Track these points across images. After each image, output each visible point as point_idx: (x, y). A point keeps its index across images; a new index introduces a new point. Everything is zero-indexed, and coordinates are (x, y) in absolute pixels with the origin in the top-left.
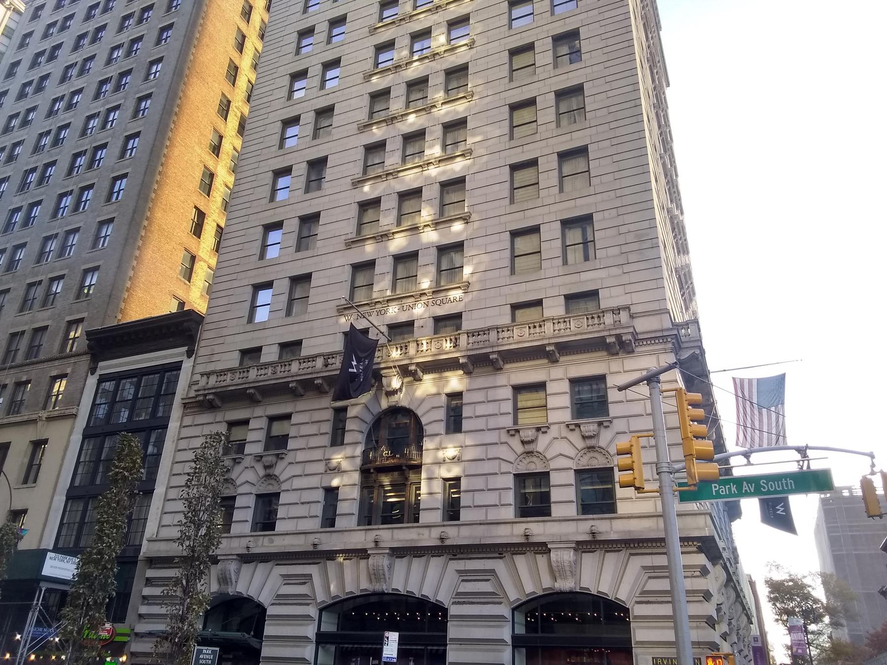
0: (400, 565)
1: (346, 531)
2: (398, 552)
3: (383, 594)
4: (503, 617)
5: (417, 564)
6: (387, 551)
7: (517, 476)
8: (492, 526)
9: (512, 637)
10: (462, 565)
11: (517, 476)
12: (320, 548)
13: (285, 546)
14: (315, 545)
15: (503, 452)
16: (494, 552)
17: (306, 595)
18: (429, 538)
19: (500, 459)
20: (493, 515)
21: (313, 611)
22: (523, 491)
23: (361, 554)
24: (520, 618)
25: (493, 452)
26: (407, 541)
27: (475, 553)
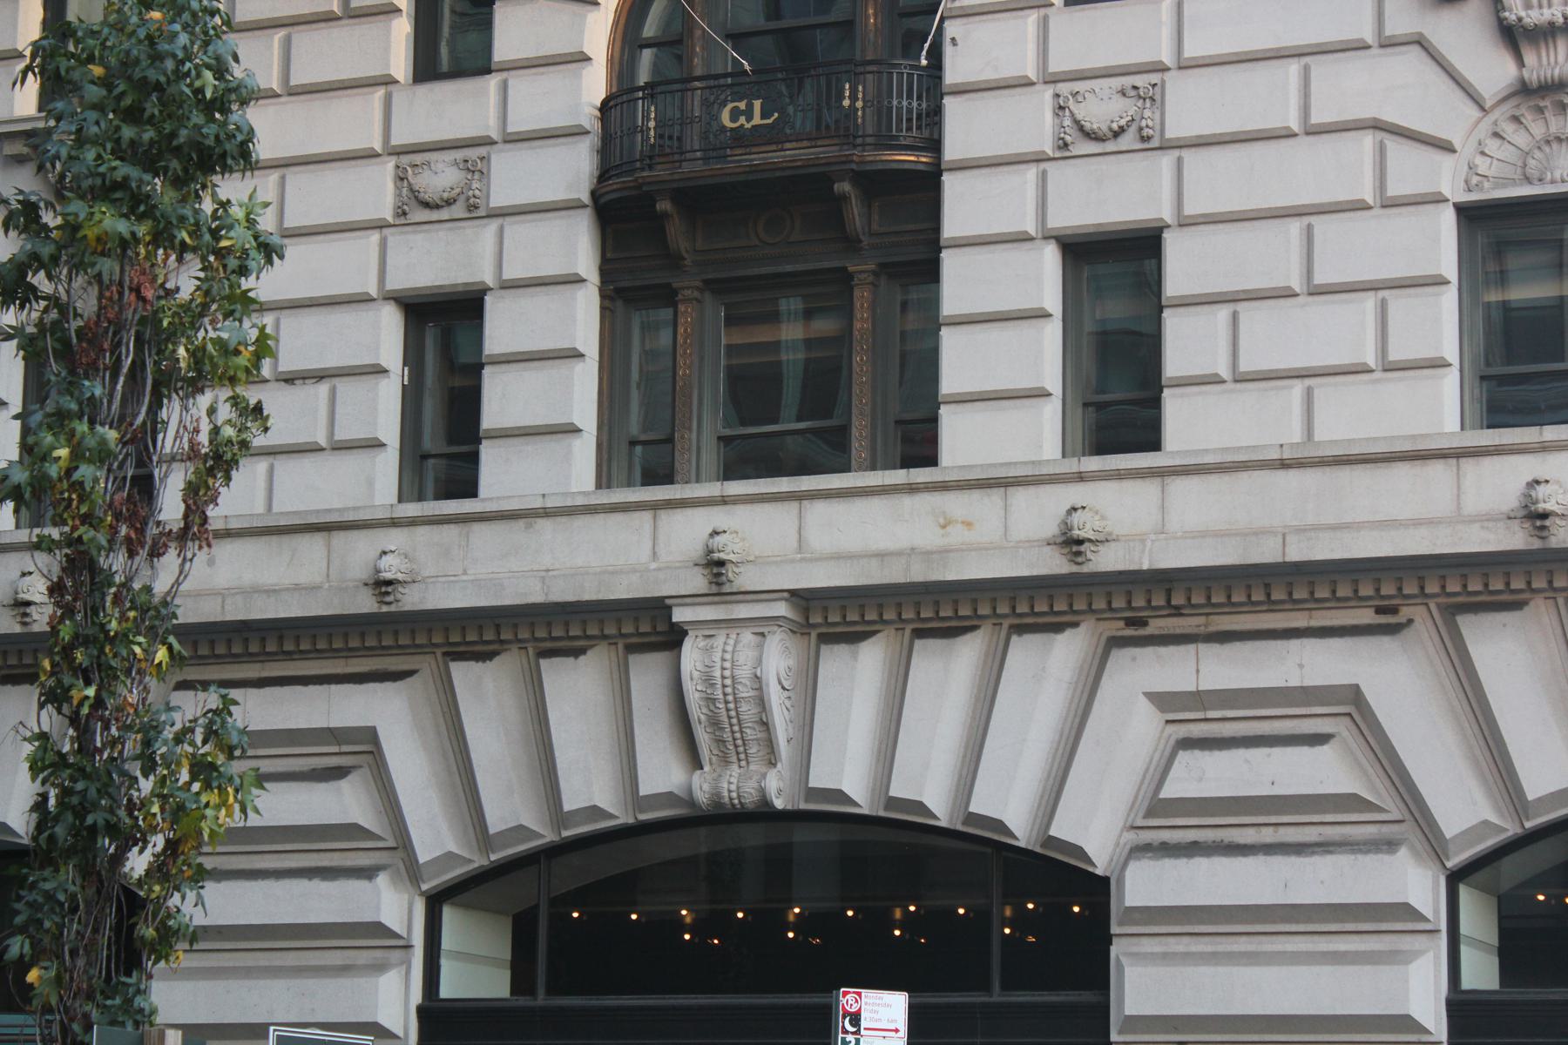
0: (856, 674)
1: (546, 513)
2: (832, 617)
3: (764, 814)
4: (1405, 911)
5: (947, 672)
6: (781, 609)
7: (1472, 216)
8: (1345, 474)
9: (1450, 1004)
10: (1178, 669)
11: (1472, 216)
12: (412, 600)
13: (222, 594)
14: (382, 586)
15: (1401, 89)
16: (1357, 599)
17: (352, 831)
18: (1000, 539)
19: (1377, 126)
20: (1347, 417)
21: (394, 905)
22: (1494, 296)
23: (648, 627)
24: (1477, 919)
25: (1347, 89)
26: (881, 556)
27: (1251, 606)
